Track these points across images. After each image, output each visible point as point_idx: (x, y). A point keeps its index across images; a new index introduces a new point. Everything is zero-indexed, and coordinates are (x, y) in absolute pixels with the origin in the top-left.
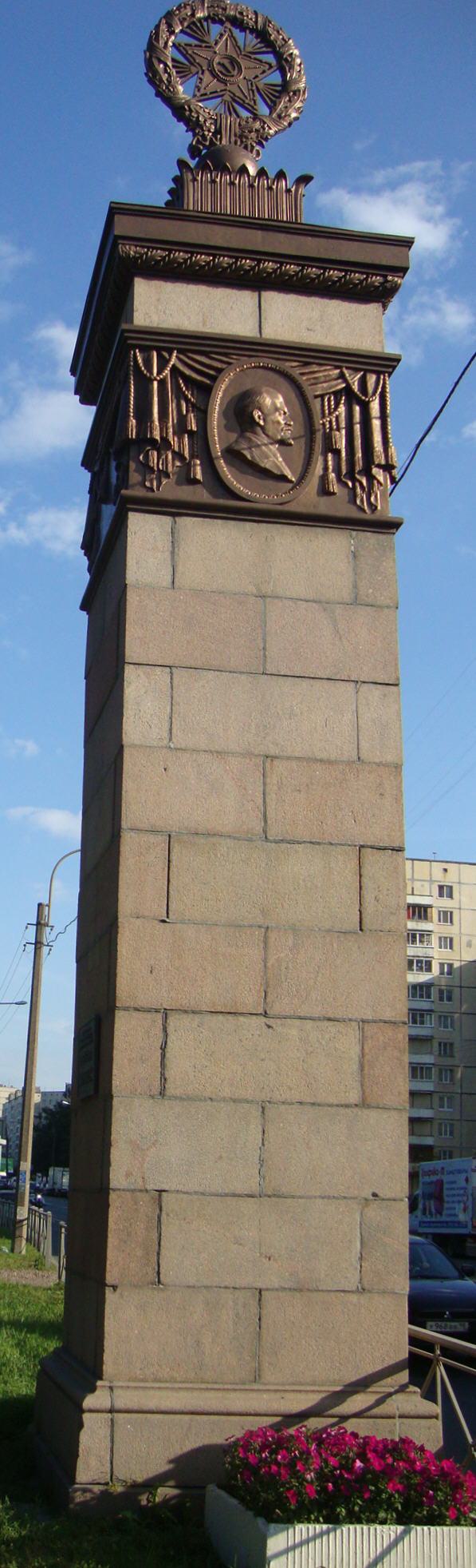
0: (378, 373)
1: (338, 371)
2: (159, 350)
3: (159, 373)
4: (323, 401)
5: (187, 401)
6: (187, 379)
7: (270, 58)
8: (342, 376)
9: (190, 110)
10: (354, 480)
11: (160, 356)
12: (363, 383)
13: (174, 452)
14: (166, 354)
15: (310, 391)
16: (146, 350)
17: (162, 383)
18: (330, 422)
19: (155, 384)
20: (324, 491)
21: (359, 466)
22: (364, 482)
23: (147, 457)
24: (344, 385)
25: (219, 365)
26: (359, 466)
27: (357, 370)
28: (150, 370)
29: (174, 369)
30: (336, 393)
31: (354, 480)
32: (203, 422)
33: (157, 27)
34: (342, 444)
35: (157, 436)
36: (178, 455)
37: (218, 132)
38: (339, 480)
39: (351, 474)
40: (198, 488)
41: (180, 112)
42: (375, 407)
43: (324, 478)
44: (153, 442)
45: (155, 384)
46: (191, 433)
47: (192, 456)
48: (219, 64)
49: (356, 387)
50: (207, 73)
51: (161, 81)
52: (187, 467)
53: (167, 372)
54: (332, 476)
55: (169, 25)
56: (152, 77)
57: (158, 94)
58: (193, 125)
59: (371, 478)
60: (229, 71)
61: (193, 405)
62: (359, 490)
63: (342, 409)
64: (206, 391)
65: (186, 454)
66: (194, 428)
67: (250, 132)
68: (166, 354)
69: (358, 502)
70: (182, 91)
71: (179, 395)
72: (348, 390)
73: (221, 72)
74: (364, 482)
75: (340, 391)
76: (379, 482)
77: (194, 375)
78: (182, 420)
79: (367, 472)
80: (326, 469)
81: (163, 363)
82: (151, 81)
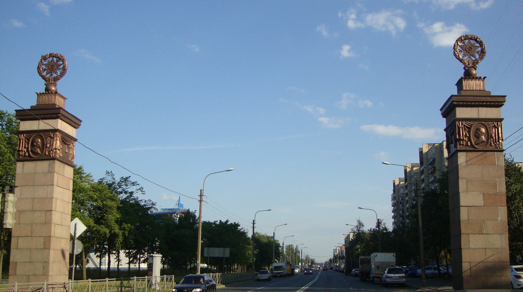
0: (500, 122)
1: (492, 122)
2: (461, 121)
6: (466, 126)
7: (478, 45)
9: (463, 61)
10: (496, 143)
11: (461, 123)
12: (497, 124)
13: (465, 141)
14: (462, 122)
15: (488, 127)
16: (459, 121)
17: (462, 128)
18: (492, 132)
19: (461, 128)
20: (491, 145)
21: (497, 140)
22: (498, 143)
23: (460, 142)
26: (497, 140)
27: (496, 122)
28: (460, 125)
29: (464, 125)
30: (493, 127)
31: (496, 143)
32: (469, 135)
33: (455, 44)
35: (462, 138)
36: (466, 141)
37: (469, 64)
38: (494, 143)
39: (496, 142)
40: (469, 147)
41: (461, 61)
42: (500, 129)
43: (491, 143)
44: (461, 140)
45: (461, 128)
46: (468, 137)
47: (468, 141)
49: (496, 125)
50: (465, 51)
52: (467, 143)
53: (463, 126)
54: (492, 142)
57: (456, 58)
58: (464, 64)
59: (499, 142)
61: (468, 131)
62: (497, 145)
63: (494, 129)
64: (470, 128)
65: (467, 141)
66: (468, 136)
68: (462, 122)
71: (465, 130)
72: (495, 126)
74: (498, 143)
77: (467, 125)
78: (466, 134)
79: (498, 141)
80: (491, 141)
81: (462, 124)
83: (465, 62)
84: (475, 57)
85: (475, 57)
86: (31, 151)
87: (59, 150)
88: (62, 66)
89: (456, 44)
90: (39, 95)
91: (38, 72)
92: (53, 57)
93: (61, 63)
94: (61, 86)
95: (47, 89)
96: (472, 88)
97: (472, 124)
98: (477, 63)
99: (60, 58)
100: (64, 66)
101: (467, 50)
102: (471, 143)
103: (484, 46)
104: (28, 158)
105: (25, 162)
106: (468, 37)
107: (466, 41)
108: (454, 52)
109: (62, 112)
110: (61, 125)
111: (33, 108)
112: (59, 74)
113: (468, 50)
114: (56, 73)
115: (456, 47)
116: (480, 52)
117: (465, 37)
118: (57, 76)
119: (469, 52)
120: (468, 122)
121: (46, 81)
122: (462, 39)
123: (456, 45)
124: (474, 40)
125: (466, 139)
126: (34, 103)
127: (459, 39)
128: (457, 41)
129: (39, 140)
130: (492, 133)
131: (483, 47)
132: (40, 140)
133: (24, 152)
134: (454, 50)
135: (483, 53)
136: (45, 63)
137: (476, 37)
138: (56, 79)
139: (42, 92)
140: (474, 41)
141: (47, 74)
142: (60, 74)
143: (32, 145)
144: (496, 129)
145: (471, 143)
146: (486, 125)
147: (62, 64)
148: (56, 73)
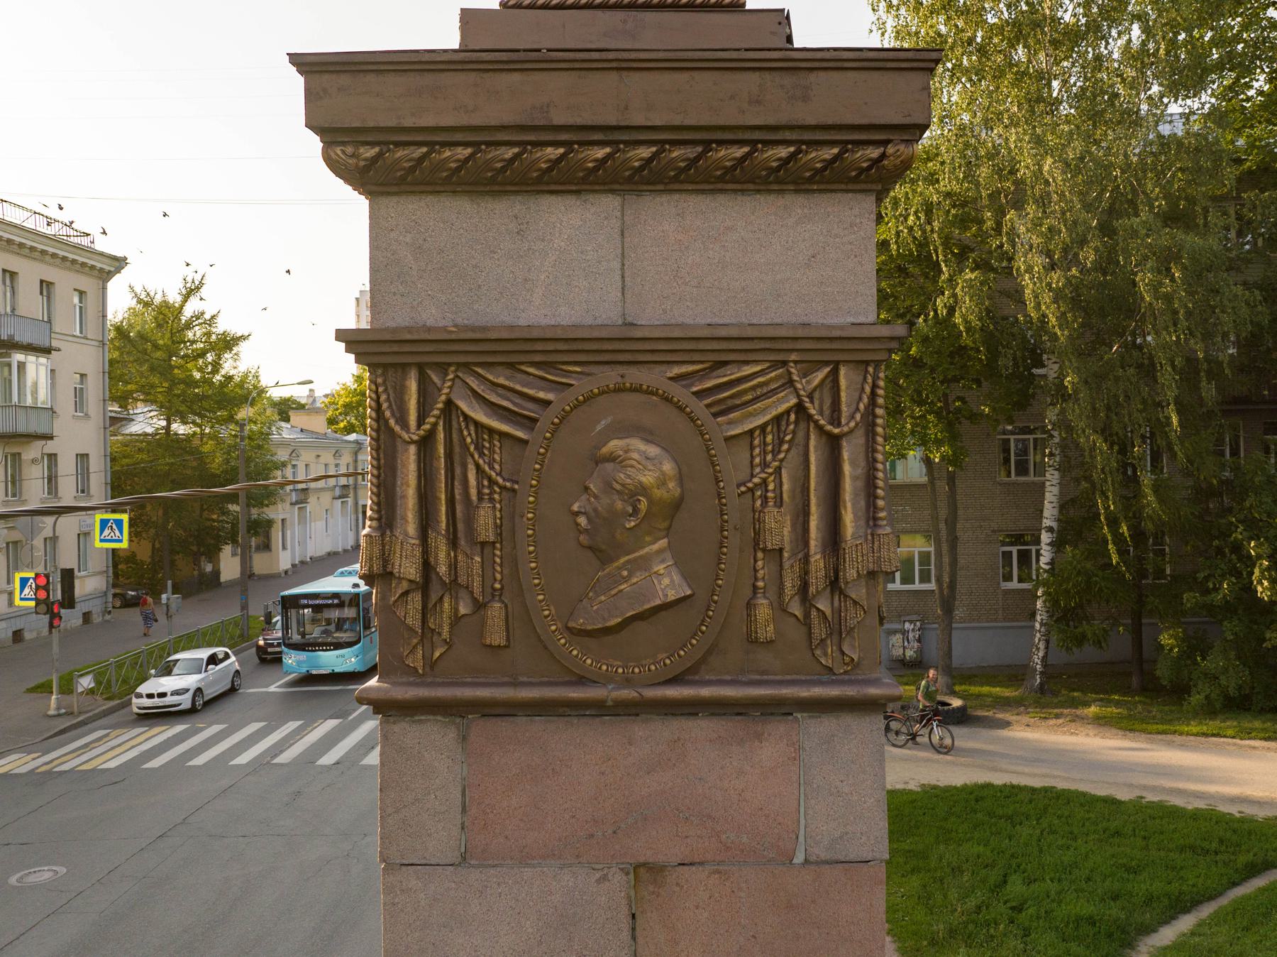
2: (421, 368)
3: (420, 422)
4: (752, 438)
8: (791, 382)
17: (426, 443)
19: (413, 449)
24: (794, 401)
25: (529, 410)
27: (827, 363)
34: (779, 528)
69: (818, 652)
72: (800, 408)
75: (788, 412)
79: (835, 584)
130: (765, 499)
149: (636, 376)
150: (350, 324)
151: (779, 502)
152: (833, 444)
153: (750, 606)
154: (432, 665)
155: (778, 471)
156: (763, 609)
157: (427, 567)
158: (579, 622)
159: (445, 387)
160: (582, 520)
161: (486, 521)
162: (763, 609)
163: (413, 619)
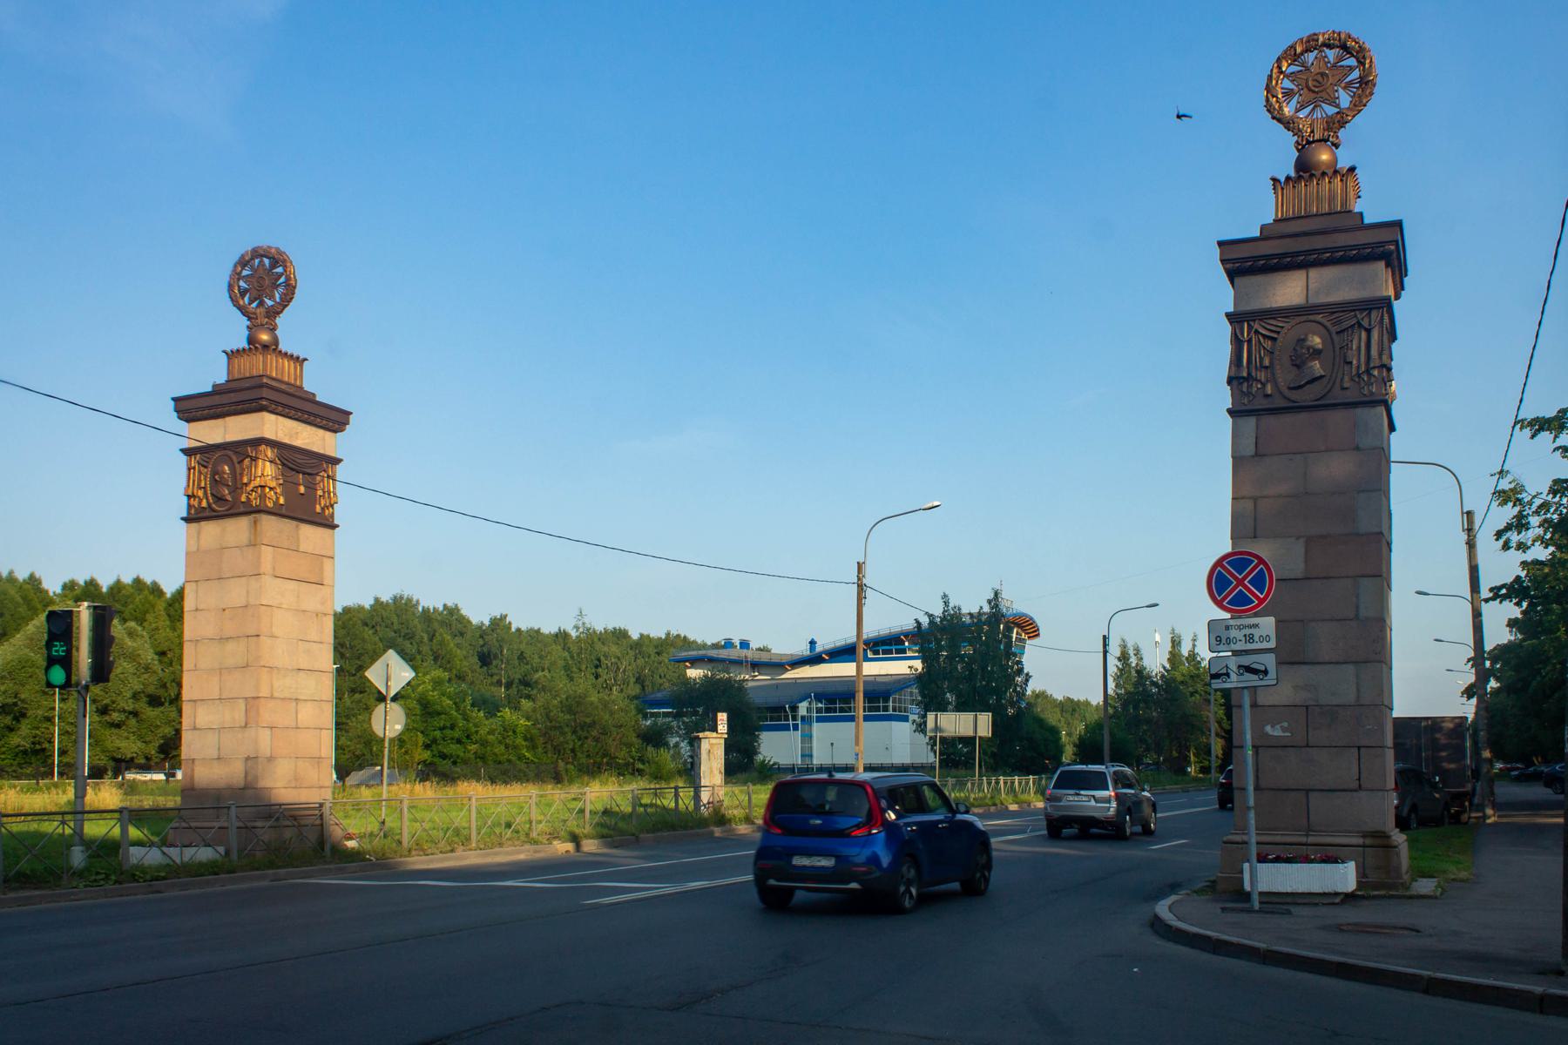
2: (1247, 321)
3: (1248, 335)
5: (1264, 348)
6: (1264, 336)
8: (1356, 316)
11: (1249, 325)
14: (1252, 323)
22: (1366, 379)
23: (1242, 387)
25: (1278, 329)
27: (1366, 309)
37: (1312, 132)
41: (1288, 124)
46: (1266, 367)
48: (1314, 80)
50: (1305, 89)
51: (1274, 109)
55: (1279, 67)
56: (1269, 108)
58: (1297, 132)
60: (1320, 83)
67: (1334, 123)
68: (1252, 323)
70: (1288, 110)
72: (1358, 323)
73: (1314, 86)
76: (1374, 376)
77: (1264, 332)
79: (1368, 372)
82: (1269, 111)
83: (1301, 126)
84: (1337, 106)
85: (1337, 106)
86: (212, 494)
87: (271, 489)
88: (282, 279)
89: (1275, 71)
90: (232, 355)
91: (231, 297)
92: (262, 256)
93: (280, 270)
94: (291, 331)
95: (251, 340)
96: (1305, 209)
97: (1282, 327)
98: (1343, 124)
99: (278, 259)
100: (288, 279)
101: (1310, 84)
102: (1276, 385)
103: (1368, 61)
104: (208, 513)
105: (203, 523)
106: (1317, 40)
107: (1310, 54)
108: (1267, 100)
109: (265, 393)
110: (273, 426)
111: (218, 390)
112: (278, 299)
113: (1316, 89)
114: (272, 297)
115: (1274, 82)
116: (1358, 85)
117: (1308, 41)
118: (272, 306)
119: (1317, 93)
120: (1268, 321)
121: (250, 319)
122: (1295, 50)
123: (1274, 76)
124: (1338, 47)
125: (1261, 376)
126: (222, 378)
127: (1285, 52)
128: (1279, 60)
129: (226, 468)
131: (1367, 66)
132: (229, 467)
133: (199, 497)
134: (1267, 93)
135: (1365, 85)
136: (245, 273)
137: (1343, 36)
138: (274, 313)
139: (241, 347)
140: (1338, 50)
141: (251, 302)
142: (281, 298)
143: (215, 482)
144: (1364, 334)
145: (1276, 385)
146: (1328, 324)
147: (283, 274)
148: (272, 297)
149: (1311, 317)
150: (1231, 309)
151: (1352, 349)
152: (1369, 331)
153: (1342, 380)
154: (1249, 401)
155: (1352, 341)
156: (1346, 378)
157: (1249, 374)
158: (1292, 385)
159: (1256, 326)
160: (1293, 358)
161: (1267, 362)
162: (1346, 378)
163: (1245, 389)
